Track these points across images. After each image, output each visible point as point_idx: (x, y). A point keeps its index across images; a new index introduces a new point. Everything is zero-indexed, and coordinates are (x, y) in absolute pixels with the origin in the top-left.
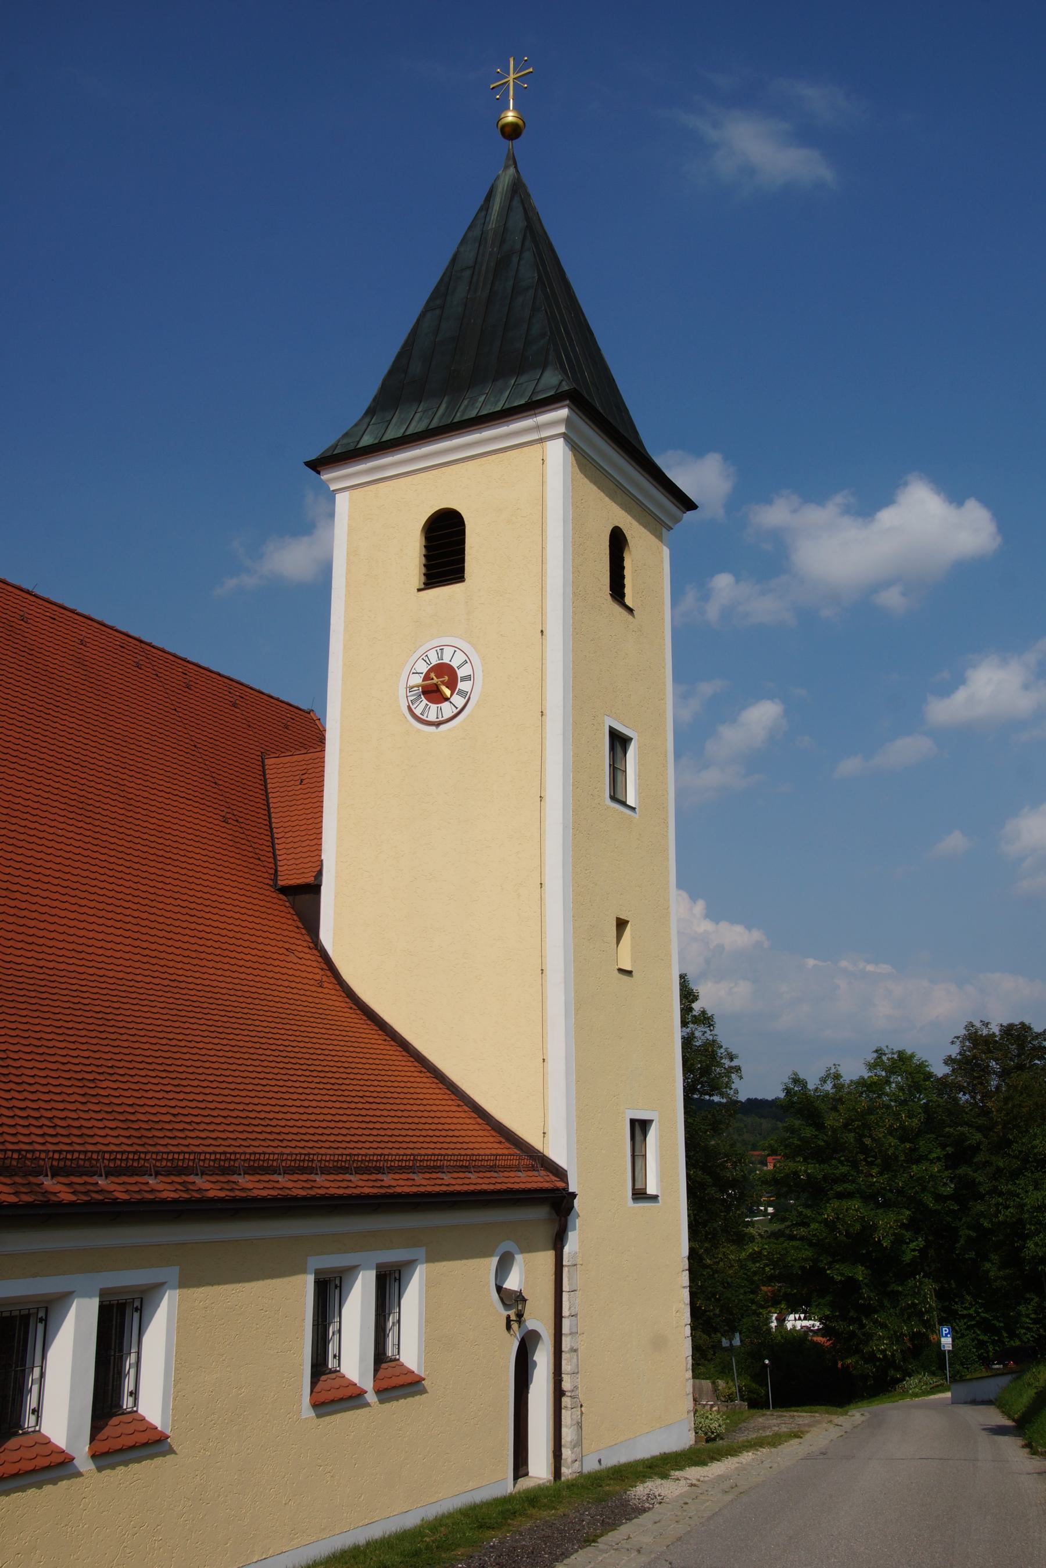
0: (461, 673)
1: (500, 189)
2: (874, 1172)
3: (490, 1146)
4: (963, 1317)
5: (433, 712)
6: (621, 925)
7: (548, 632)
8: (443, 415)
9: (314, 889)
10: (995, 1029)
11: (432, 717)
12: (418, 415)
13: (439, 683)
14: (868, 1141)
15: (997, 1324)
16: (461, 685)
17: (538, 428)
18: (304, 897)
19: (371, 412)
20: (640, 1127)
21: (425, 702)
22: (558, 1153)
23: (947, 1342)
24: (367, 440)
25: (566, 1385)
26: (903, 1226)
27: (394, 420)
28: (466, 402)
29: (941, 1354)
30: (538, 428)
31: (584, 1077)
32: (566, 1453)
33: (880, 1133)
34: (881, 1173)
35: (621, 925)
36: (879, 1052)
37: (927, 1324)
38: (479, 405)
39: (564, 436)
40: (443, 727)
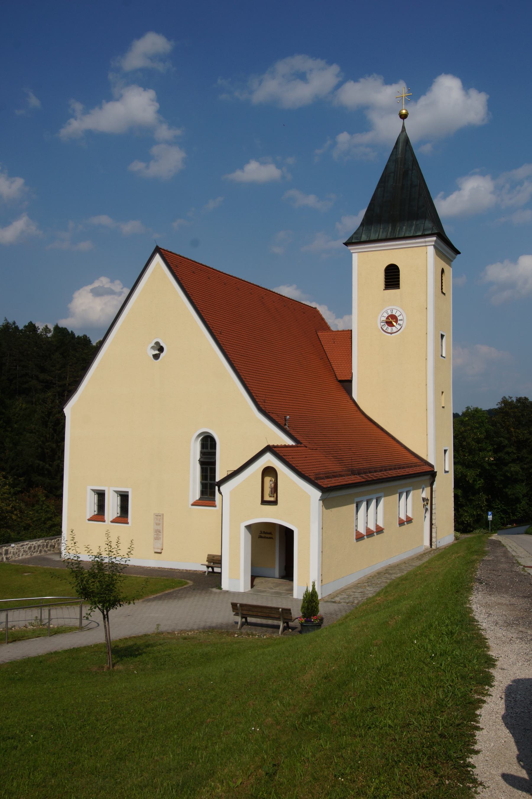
0: (399, 318)
1: (401, 141)
2: (467, 455)
3: (416, 460)
4: (496, 508)
5: (390, 329)
6: (443, 392)
8: (391, 232)
9: (350, 381)
10: (514, 400)
11: (389, 331)
12: (381, 230)
13: (391, 321)
14: (465, 443)
15: (509, 511)
16: (399, 322)
17: (425, 242)
19: (362, 224)
20: (445, 451)
21: (387, 326)
22: (431, 461)
23: (490, 517)
24: (364, 238)
25: (433, 522)
26: (477, 475)
27: (372, 230)
28: (398, 228)
29: (487, 521)
30: (425, 242)
31: (437, 438)
32: (433, 540)
33: (469, 440)
34: (469, 455)
35: (443, 392)
36: (468, 408)
37: (482, 511)
38: (404, 230)
39: (434, 245)
40: (393, 335)
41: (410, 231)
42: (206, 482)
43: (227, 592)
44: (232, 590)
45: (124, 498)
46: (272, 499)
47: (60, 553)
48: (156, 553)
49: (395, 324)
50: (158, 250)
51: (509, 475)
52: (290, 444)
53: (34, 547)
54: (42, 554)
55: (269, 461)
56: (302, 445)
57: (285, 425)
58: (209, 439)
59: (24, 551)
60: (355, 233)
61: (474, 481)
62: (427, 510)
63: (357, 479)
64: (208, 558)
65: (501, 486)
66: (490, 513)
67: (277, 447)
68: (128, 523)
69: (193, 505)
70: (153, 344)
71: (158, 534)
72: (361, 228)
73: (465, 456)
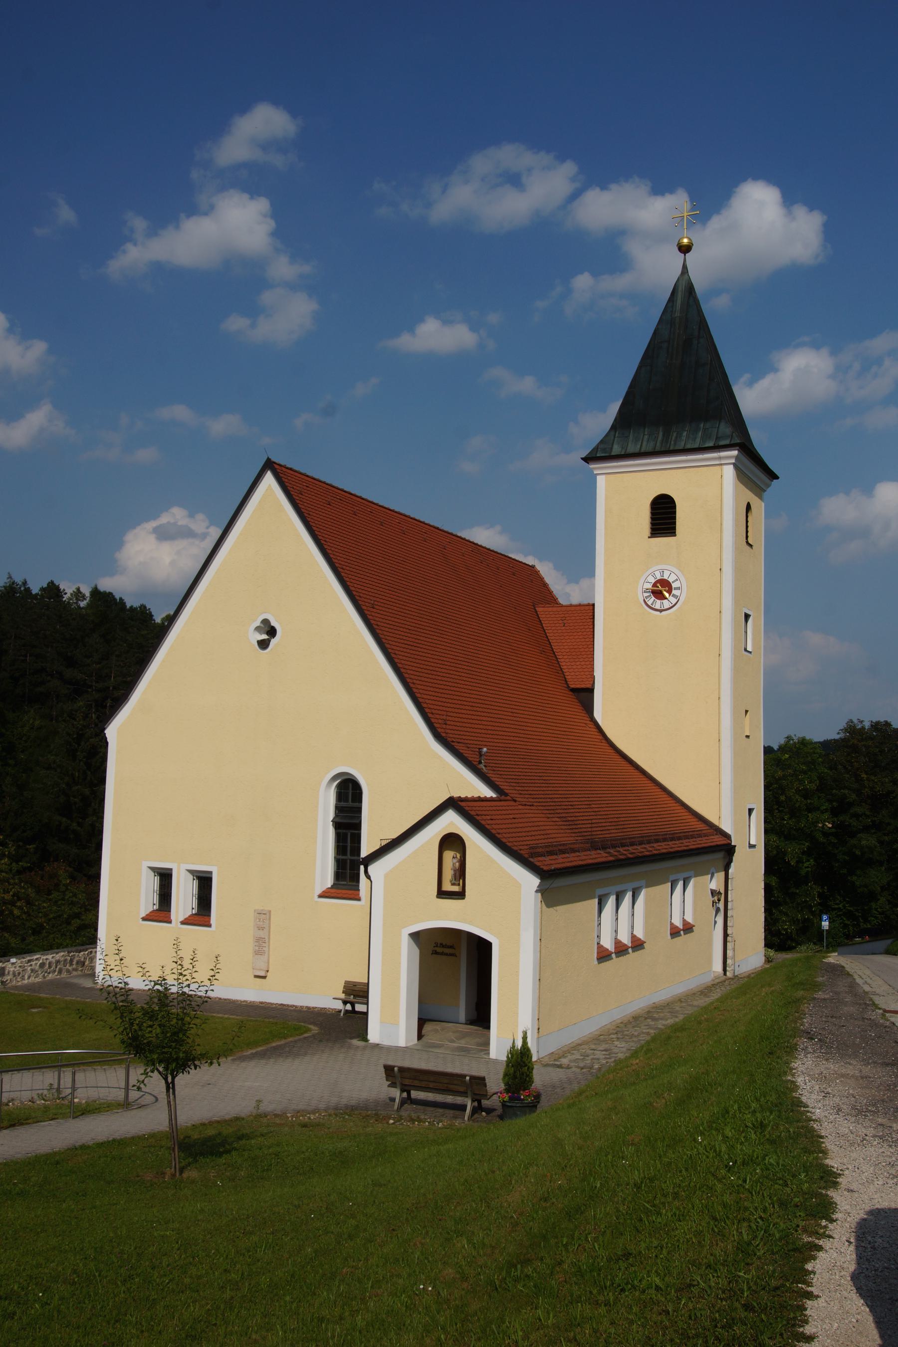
0: (674, 585)
1: (680, 289)
2: (786, 817)
3: (701, 826)
4: (834, 909)
5: (658, 604)
6: (747, 712)
7: (724, 569)
8: (662, 441)
9: (591, 691)
10: (867, 725)
11: (658, 606)
12: (646, 437)
13: (661, 589)
14: (783, 798)
15: (857, 914)
16: (674, 592)
17: (720, 458)
18: (584, 695)
19: (614, 427)
20: (750, 811)
22: (726, 827)
23: (825, 924)
24: (616, 450)
25: (729, 932)
26: (803, 853)
29: (820, 931)
30: (720, 458)
32: (729, 961)
34: (790, 818)
35: (747, 712)
36: (789, 738)
37: (812, 913)
39: (734, 464)
42: (344, 857)
43: (377, 1046)
44: (386, 1042)
45: (204, 882)
46: (456, 889)
47: (93, 975)
48: (256, 977)
49: (667, 595)
50: (269, 465)
51: (858, 852)
52: (488, 796)
53: (50, 963)
54: (62, 976)
55: (452, 823)
56: (508, 798)
57: (480, 762)
58: (351, 785)
59: (32, 970)
60: (602, 442)
61: (797, 862)
62: (718, 910)
63: (601, 856)
64: (345, 987)
65: (845, 871)
66: (825, 917)
67: (466, 800)
68: (209, 926)
69: (320, 896)
70: (258, 623)
71: (261, 945)
72: (612, 433)
73: (784, 819)
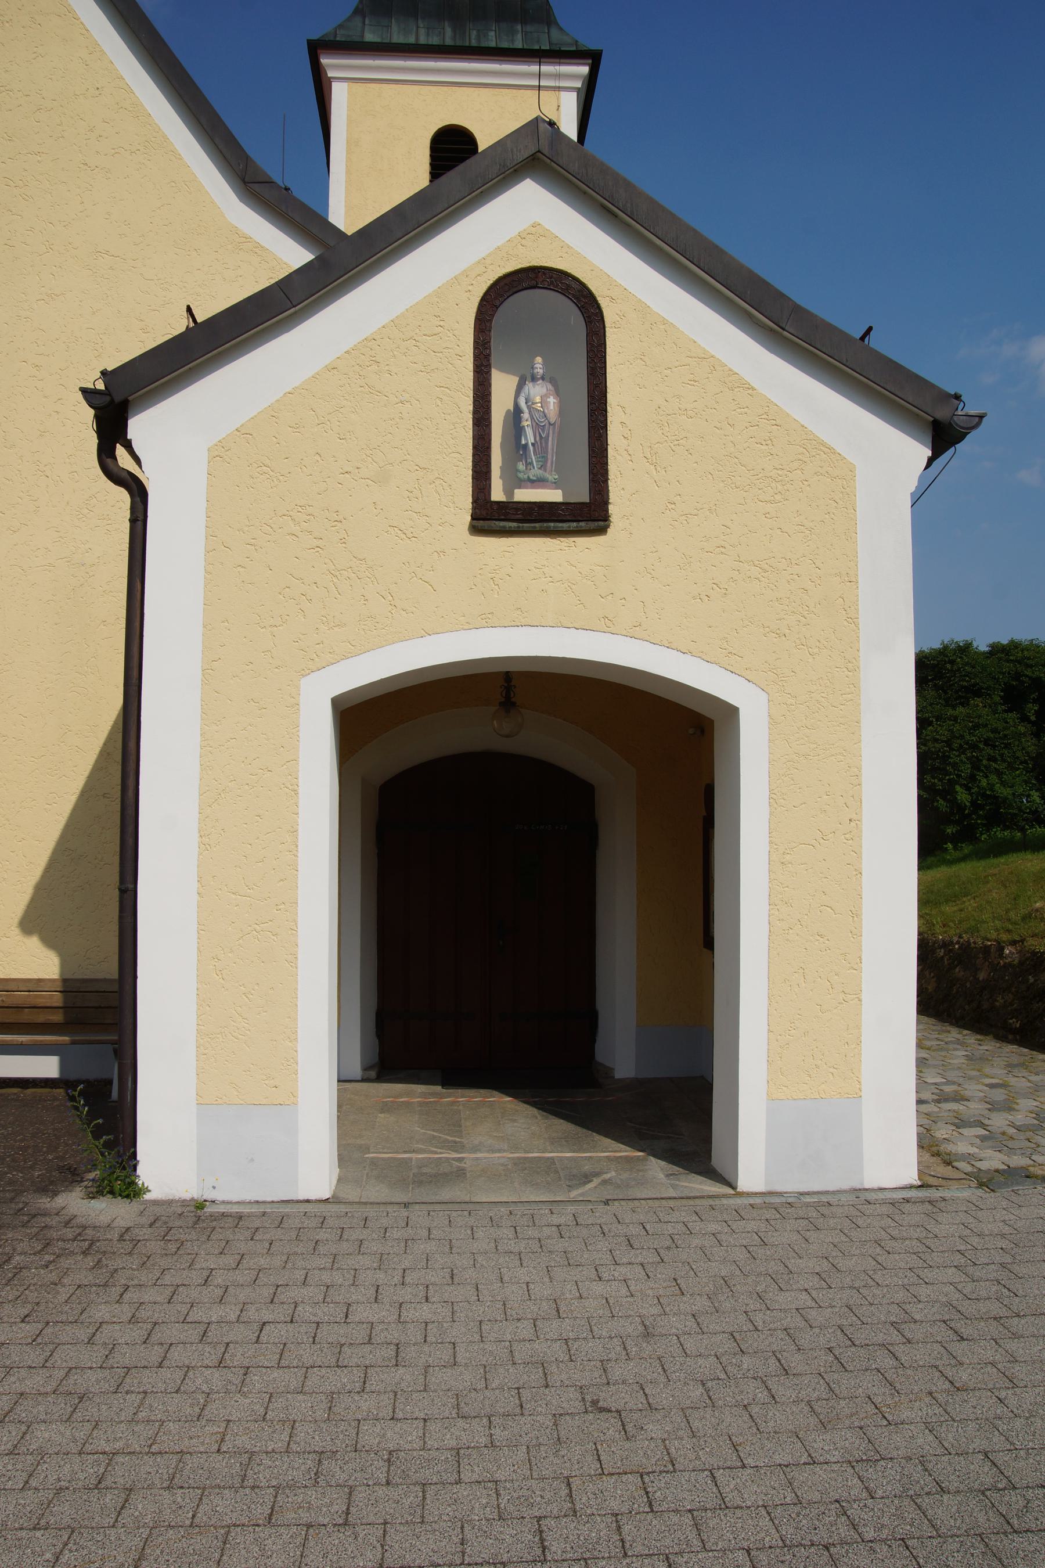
17: (558, 76)
30: (558, 76)
39: (578, 90)
41: (513, 41)
43: (197, 1213)
44: (232, 1189)
